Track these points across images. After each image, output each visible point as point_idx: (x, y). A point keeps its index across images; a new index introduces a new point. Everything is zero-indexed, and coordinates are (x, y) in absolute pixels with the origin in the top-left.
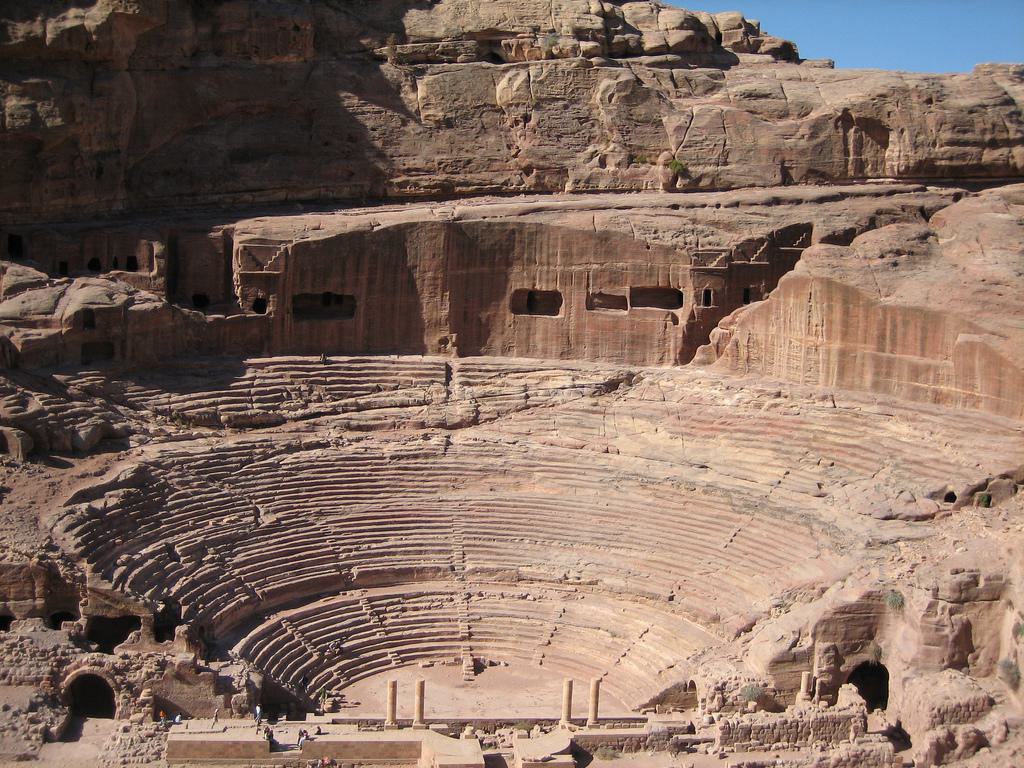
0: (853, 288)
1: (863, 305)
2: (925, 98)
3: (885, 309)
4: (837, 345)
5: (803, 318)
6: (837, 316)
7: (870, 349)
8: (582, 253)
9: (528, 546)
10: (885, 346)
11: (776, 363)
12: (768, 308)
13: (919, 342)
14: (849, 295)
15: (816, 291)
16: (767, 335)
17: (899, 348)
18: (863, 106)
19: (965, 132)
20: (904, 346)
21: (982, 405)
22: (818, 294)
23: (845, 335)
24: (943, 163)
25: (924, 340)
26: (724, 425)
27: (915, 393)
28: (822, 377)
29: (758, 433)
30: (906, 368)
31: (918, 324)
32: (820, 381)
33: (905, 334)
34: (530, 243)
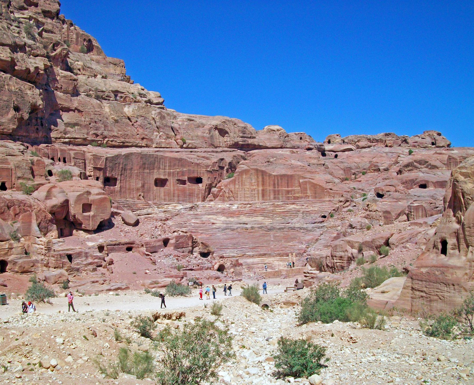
3: (274, 176)
4: (261, 188)
6: (260, 179)
7: (271, 188)
8: (175, 165)
14: (263, 173)
18: (220, 124)
19: (244, 134)
21: (310, 198)
23: (263, 185)
24: (241, 143)
25: (288, 183)
27: (288, 198)
28: (257, 198)
29: (253, 213)
30: (284, 192)
33: (281, 183)
34: (160, 162)
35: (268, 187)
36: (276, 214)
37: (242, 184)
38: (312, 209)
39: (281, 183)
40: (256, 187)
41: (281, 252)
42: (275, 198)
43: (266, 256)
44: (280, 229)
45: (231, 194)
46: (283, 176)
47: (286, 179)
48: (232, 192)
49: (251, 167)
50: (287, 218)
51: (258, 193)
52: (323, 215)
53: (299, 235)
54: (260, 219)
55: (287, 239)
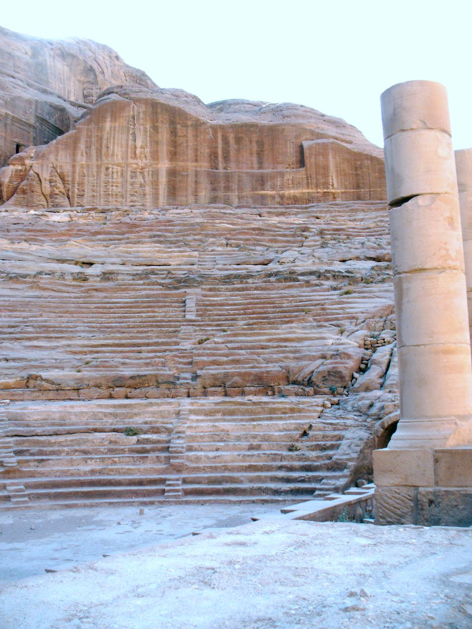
0: (180, 109)
2: (114, 55)
3: (215, 129)
4: (164, 165)
5: (124, 143)
6: (164, 135)
7: (204, 166)
10: (218, 164)
11: (88, 193)
12: (76, 140)
15: (139, 113)
16: (74, 166)
20: (238, 162)
22: (142, 115)
23: (174, 155)
25: (260, 154)
26: (72, 231)
27: (262, 200)
28: (149, 199)
29: (123, 234)
30: (246, 180)
31: (254, 139)
32: (148, 204)
35: (191, 165)
36: (214, 236)
37: (99, 151)
38: (352, 224)
39: (238, 150)
41: (231, 369)
42: (214, 200)
43: (152, 391)
44: (228, 279)
45: (60, 184)
47: (254, 139)
48: (62, 178)
49: (133, 95)
50: (258, 248)
51: (155, 184)
53: (318, 296)
54: (148, 250)
55: (262, 315)
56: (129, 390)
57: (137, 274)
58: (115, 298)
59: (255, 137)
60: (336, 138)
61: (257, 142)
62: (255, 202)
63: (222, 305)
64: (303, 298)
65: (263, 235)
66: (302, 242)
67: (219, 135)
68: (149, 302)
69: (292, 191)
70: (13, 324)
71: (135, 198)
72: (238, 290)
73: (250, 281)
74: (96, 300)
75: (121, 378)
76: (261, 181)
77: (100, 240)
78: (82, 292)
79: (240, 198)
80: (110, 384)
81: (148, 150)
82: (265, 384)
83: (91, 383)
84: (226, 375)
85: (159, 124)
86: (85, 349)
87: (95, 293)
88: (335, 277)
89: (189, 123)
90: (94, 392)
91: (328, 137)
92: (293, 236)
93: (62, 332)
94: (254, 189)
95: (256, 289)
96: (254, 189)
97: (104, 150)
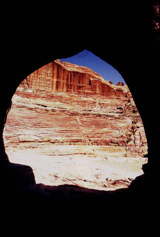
0: (60, 65)
1: (63, 70)
3: (68, 72)
4: (55, 80)
5: (45, 72)
6: (55, 72)
7: (65, 81)
9: (10, 128)
13: (78, 80)
17: (72, 82)
20: (73, 81)
23: (58, 78)
25: (79, 80)
29: (50, 98)
30: (76, 86)
31: (78, 76)
35: (62, 80)
36: (74, 102)
39: (74, 78)
40: (51, 78)
42: (67, 91)
43: (80, 143)
44: (84, 115)
46: (75, 73)
47: (78, 76)
51: (53, 84)
52: (118, 107)
54: (58, 103)
56: (74, 143)
57: (60, 111)
58: (58, 117)
59: (78, 76)
60: (98, 79)
61: (79, 77)
62: (78, 93)
63: (86, 121)
64: (106, 122)
65: (85, 103)
66: (95, 106)
67: (69, 73)
68: (67, 119)
69: (87, 91)
70: (38, 123)
71: (46, 88)
72: (87, 118)
73: (90, 115)
74: (54, 117)
75: (73, 140)
76: (79, 88)
77: (45, 99)
78: (49, 115)
79: (74, 91)
80: (70, 141)
81: (51, 75)
82: (107, 143)
83: (66, 141)
84: (97, 140)
85: (54, 68)
86: (61, 131)
87: (52, 115)
88: (110, 117)
89: (62, 69)
90: (67, 143)
91: (97, 78)
92: (93, 104)
93: (51, 126)
94: (78, 89)
95: (92, 118)
96: (78, 89)
97: (39, 73)
